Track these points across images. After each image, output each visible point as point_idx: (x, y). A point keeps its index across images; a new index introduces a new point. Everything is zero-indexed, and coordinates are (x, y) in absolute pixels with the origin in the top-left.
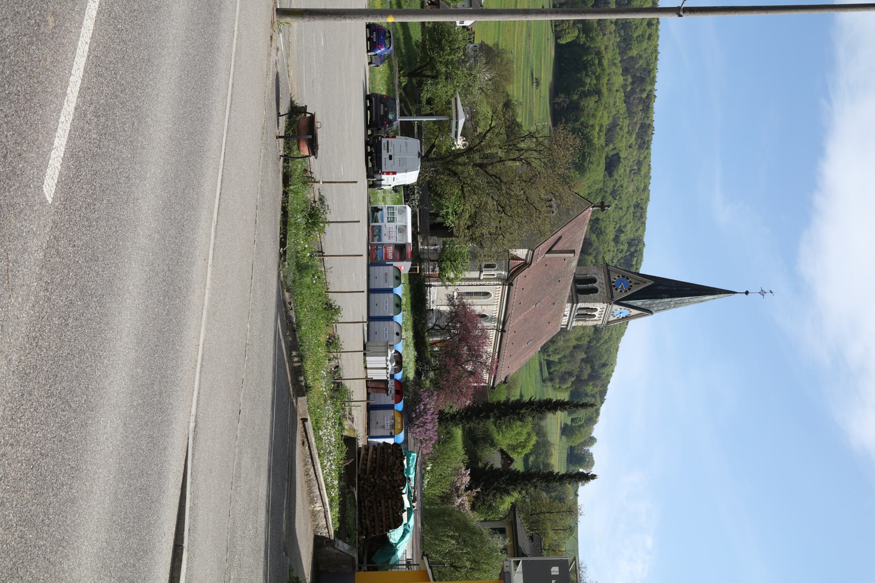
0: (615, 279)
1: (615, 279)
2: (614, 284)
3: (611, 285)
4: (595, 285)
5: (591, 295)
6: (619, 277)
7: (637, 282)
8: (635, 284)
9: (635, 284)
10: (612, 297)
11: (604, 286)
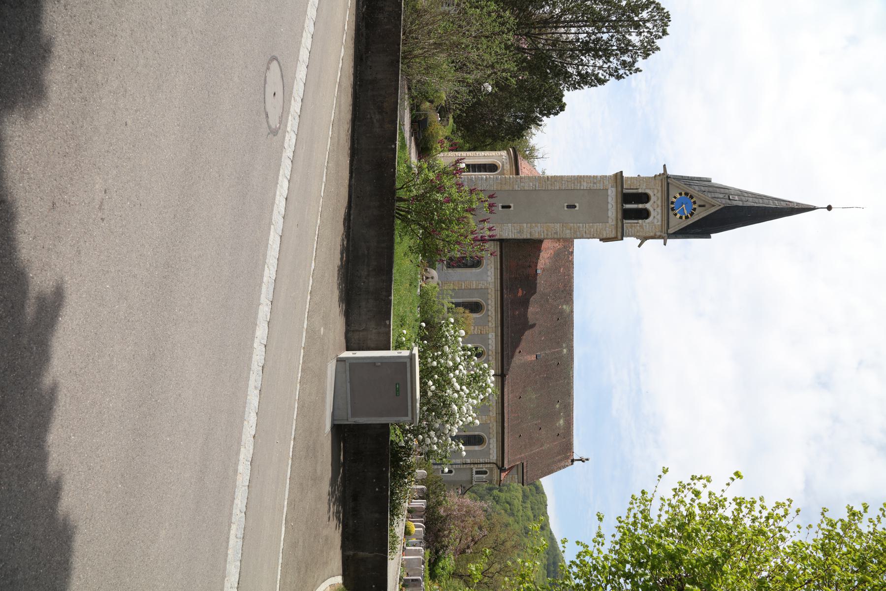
0: (675, 197)
1: (675, 197)
2: (673, 206)
3: (669, 207)
4: (648, 206)
5: (640, 221)
6: (680, 194)
7: (702, 203)
8: (700, 206)
9: (700, 206)
10: (668, 227)
11: (659, 210)
